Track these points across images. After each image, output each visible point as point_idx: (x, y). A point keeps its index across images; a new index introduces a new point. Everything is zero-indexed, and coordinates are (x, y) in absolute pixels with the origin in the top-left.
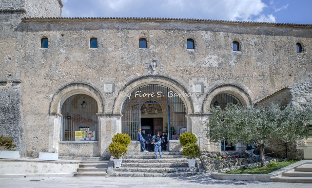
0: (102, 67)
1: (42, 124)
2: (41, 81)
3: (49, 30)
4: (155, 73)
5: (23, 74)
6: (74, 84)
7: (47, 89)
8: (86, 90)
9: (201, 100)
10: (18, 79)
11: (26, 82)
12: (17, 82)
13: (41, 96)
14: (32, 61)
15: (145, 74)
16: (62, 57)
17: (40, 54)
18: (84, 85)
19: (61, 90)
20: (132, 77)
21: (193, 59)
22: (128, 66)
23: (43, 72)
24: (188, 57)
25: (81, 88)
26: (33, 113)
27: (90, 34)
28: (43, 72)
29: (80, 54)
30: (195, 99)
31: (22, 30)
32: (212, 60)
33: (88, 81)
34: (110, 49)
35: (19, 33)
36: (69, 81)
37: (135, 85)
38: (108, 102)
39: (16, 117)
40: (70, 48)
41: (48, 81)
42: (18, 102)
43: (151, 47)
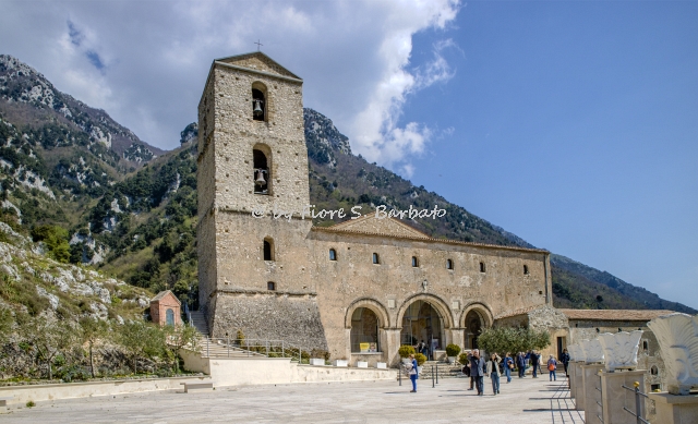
0: (385, 284)
1: (340, 336)
2: (335, 295)
3: (337, 241)
4: (425, 292)
5: (318, 287)
6: (364, 299)
7: (341, 303)
8: (372, 305)
9: (459, 316)
10: (313, 291)
11: (322, 294)
12: (314, 295)
13: (336, 309)
14: (325, 273)
15: (419, 292)
16: (352, 270)
17: (331, 267)
18: (372, 300)
19: (353, 304)
20: (409, 294)
21: (452, 279)
22: (405, 284)
23: (336, 285)
24: (448, 277)
25: (369, 302)
26: (330, 326)
27: (373, 249)
28: (336, 285)
29: (367, 270)
30: (454, 315)
31: (312, 239)
32: (465, 280)
33: (375, 297)
34: (391, 266)
35: (309, 241)
36: (360, 296)
37: (412, 301)
38: (392, 317)
39: (321, 331)
40: (358, 264)
41: (341, 295)
42: (319, 316)
43: (422, 266)
